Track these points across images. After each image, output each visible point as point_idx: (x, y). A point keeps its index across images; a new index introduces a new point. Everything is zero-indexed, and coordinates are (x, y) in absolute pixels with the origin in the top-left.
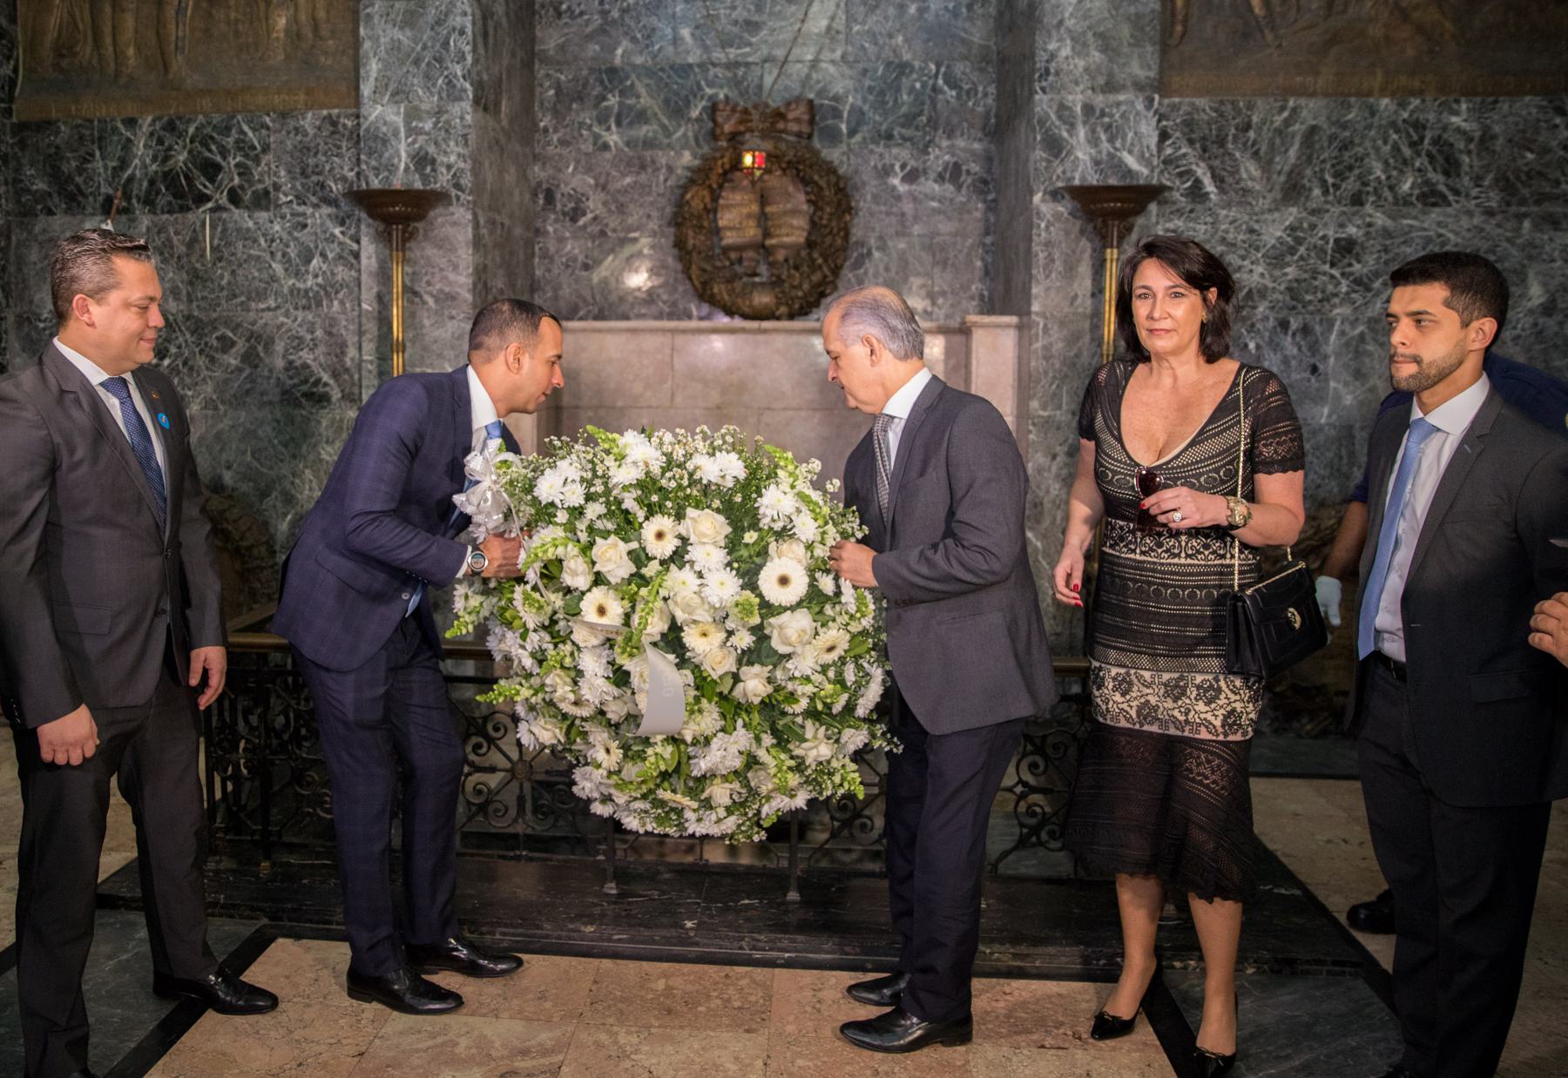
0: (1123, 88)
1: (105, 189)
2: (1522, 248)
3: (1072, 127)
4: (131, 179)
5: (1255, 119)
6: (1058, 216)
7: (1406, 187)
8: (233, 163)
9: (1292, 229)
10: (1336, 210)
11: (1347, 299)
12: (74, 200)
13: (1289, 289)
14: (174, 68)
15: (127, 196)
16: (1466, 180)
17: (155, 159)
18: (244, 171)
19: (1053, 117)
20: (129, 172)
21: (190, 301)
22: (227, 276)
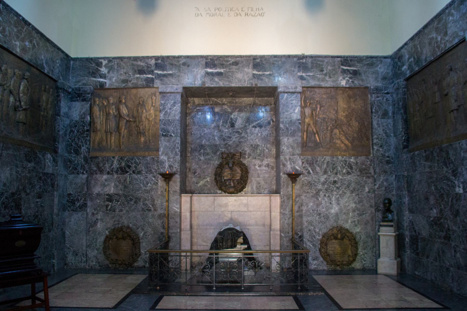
0: (295, 155)
1: (108, 170)
3: (287, 162)
4: (113, 168)
5: (318, 160)
6: (285, 177)
7: (344, 171)
8: (133, 165)
9: (326, 179)
10: (333, 175)
11: (335, 191)
12: (101, 172)
13: (326, 189)
14: (122, 148)
15: (112, 171)
16: (354, 170)
17: (118, 164)
18: (136, 167)
19: (284, 160)
20: (113, 167)
22: (132, 187)
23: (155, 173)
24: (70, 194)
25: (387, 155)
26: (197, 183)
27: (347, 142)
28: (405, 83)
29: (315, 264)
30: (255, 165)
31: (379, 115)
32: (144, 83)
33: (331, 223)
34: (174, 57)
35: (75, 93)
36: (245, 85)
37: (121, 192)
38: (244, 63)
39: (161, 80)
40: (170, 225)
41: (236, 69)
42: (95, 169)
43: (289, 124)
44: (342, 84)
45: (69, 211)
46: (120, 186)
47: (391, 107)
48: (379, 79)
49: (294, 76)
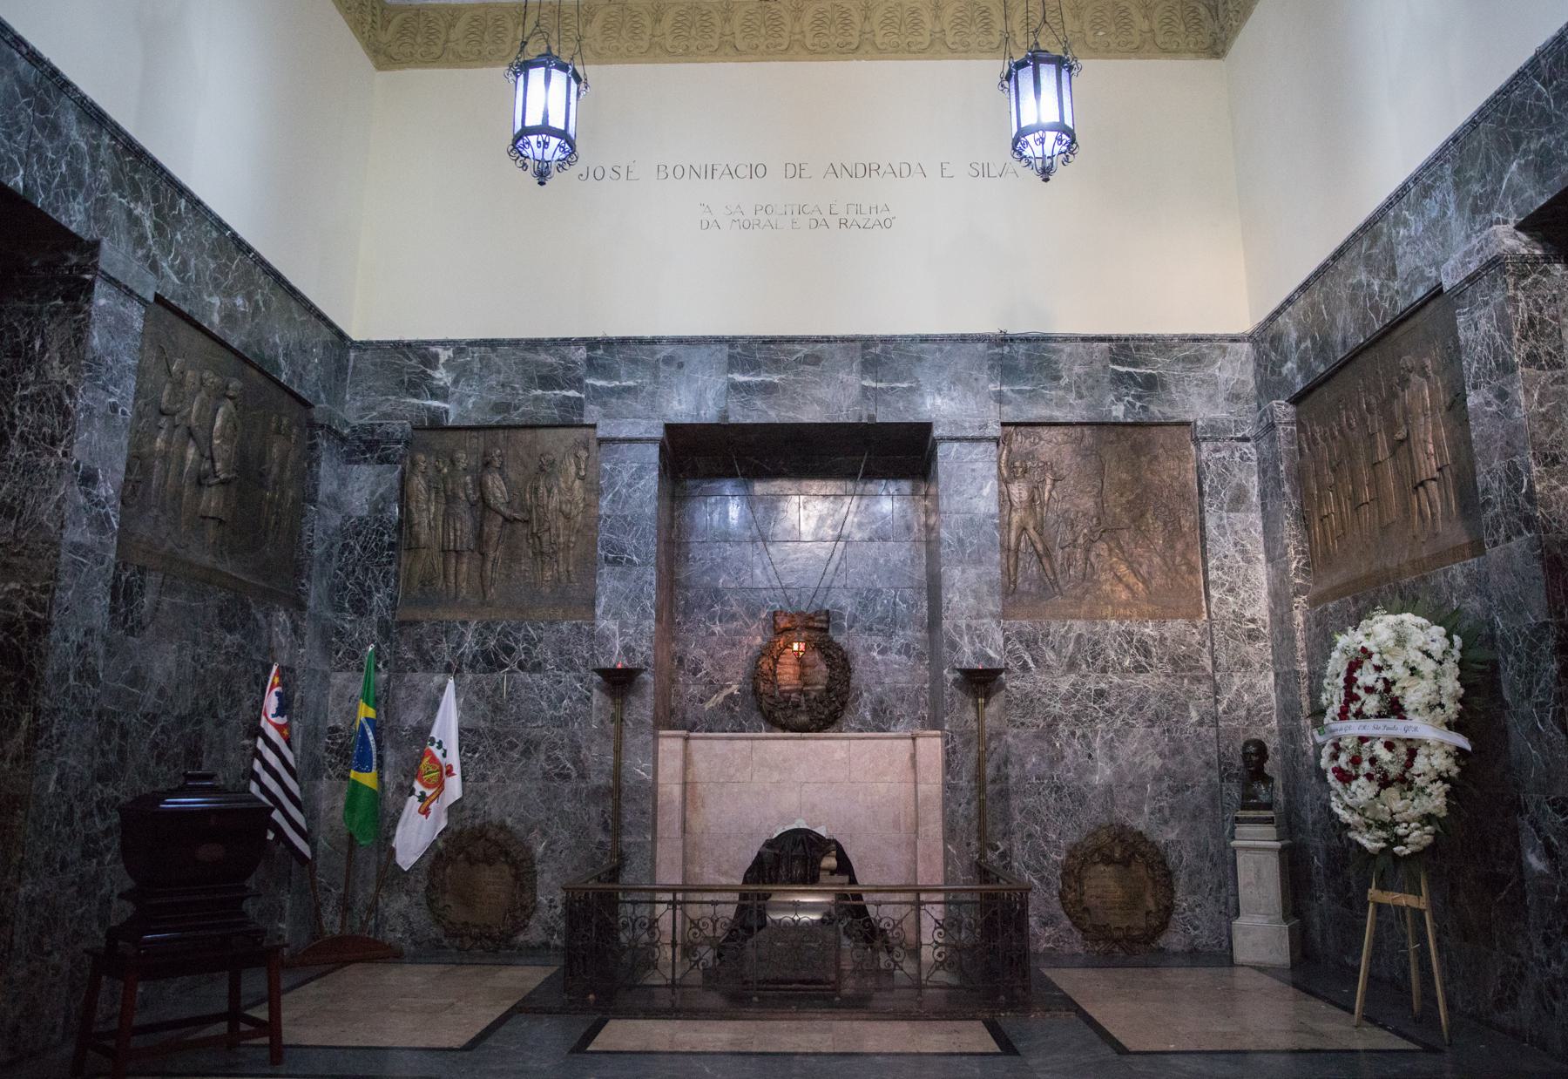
2: (1185, 693)
3: (961, 636)
4: (462, 654)
7: (1127, 663)
9: (1073, 685)
10: (1094, 675)
12: (429, 664)
17: (477, 644)
18: (527, 651)
21: (493, 721)
23: (582, 669)
24: (335, 730)
25: (1248, 614)
26: (701, 701)
27: (1132, 580)
28: (1291, 409)
29: (1049, 937)
30: (870, 648)
31: (1222, 502)
32: (556, 411)
33: (1094, 814)
34: (641, 341)
35: (360, 439)
36: (841, 420)
37: (482, 724)
38: (838, 357)
39: (604, 405)
40: (625, 821)
41: (814, 374)
42: (410, 656)
43: (964, 527)
44: (1114, 413)
45: (329, 777)
46: (482, 707)
47: (1255, 478)
48: (1220, 400)
49: (978, 393)
